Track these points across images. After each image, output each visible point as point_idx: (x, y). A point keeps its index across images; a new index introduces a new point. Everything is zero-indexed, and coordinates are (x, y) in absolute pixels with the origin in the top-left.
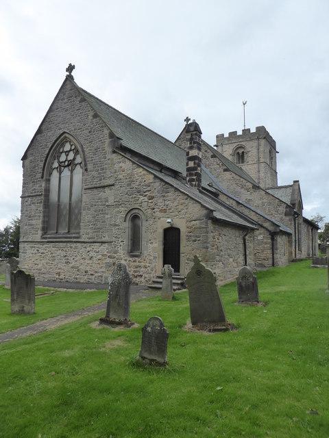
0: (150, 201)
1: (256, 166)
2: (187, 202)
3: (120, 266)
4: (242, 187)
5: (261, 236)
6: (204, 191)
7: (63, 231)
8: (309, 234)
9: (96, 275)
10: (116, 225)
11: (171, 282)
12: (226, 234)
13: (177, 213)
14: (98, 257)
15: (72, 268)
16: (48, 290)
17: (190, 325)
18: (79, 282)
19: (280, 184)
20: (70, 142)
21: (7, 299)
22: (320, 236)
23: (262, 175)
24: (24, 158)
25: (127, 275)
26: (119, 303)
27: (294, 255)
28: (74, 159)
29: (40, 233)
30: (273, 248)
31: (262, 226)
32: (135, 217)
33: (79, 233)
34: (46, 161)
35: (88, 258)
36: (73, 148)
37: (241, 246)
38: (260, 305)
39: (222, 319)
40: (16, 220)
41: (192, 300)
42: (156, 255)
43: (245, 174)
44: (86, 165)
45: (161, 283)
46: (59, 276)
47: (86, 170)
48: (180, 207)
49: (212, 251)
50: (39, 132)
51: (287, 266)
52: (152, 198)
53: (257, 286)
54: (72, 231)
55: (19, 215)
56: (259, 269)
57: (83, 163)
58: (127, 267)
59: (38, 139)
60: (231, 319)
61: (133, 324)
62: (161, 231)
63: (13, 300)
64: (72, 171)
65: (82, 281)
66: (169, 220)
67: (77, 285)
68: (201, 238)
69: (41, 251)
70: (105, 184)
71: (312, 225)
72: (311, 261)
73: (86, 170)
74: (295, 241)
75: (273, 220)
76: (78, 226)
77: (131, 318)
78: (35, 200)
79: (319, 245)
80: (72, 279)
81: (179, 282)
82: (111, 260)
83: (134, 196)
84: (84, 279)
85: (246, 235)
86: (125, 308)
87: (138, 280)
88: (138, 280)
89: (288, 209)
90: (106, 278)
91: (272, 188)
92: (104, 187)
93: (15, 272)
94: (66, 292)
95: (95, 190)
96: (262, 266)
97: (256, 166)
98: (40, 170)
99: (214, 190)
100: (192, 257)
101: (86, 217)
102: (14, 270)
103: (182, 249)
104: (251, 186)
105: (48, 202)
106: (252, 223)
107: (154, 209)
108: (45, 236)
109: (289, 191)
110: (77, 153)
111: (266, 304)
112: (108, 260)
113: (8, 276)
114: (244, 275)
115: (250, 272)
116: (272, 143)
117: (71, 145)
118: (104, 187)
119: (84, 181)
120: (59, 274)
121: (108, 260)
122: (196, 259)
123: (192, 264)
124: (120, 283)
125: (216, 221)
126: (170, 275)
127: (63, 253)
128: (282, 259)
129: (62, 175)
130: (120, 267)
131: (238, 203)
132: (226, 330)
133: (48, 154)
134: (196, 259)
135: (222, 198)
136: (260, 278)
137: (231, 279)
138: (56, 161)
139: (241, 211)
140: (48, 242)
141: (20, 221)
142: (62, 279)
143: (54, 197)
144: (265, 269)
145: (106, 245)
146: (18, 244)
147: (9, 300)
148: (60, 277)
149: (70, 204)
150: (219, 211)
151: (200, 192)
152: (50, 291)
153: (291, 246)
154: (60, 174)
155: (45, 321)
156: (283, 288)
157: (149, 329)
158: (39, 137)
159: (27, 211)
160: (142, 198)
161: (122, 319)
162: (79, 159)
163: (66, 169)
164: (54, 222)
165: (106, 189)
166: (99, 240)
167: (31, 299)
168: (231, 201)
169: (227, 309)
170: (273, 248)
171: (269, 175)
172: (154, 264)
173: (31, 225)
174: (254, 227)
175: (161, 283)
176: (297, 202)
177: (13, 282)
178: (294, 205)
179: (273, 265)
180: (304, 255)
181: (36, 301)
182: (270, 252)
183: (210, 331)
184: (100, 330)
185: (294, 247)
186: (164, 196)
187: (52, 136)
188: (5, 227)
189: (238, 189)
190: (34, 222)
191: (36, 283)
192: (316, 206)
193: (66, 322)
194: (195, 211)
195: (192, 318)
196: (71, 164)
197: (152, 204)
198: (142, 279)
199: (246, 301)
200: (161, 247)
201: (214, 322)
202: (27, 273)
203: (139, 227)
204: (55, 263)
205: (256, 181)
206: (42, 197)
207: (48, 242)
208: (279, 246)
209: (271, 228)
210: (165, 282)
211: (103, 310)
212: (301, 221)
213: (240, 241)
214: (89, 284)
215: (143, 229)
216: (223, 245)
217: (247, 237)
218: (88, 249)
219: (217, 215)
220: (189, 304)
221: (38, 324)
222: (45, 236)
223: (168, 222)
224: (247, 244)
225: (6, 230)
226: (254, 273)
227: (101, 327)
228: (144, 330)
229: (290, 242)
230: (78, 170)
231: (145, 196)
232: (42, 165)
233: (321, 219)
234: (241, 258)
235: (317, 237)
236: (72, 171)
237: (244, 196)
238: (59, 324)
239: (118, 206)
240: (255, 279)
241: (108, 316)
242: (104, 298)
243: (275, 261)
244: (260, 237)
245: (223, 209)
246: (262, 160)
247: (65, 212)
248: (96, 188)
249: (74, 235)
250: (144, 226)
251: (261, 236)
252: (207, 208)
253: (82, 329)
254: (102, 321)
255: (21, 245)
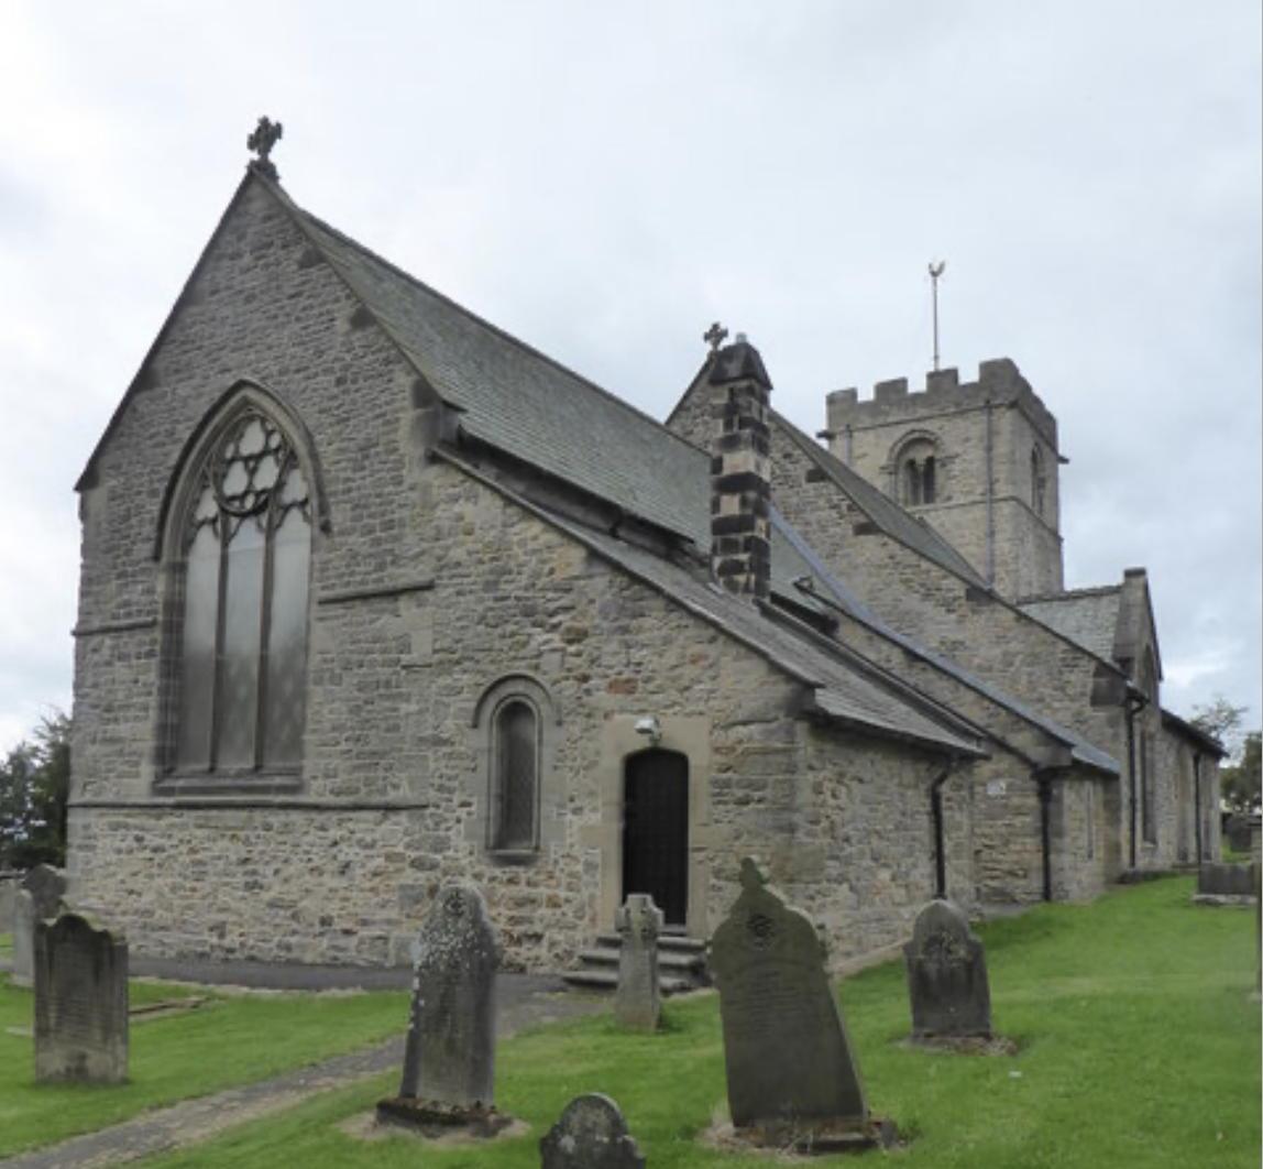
0: (572, 649)
1: (979, 512)
2: (711, 651)
3: (456, 902)
4: (927, 596)
5: (998, 782)
6: (779, 608)
7: (236, 762)
8: (1184, 778)
9: (364, 932)
10: (445, 742)
11: (653, 958)
12: (867, 777)
13: (674, 695)
14: (373, 864)
15: (272, 905)
16: (176, 992)
17: (726, 1127)
18: (297, 963)
19: (1073, 581)
20: (263, 421)
21: (21, 1026)
22: (1230, 784)
23: (1003, 546)
24: (86, 483)
25: (484, 933)
26: (451, 1045)
27: (1125, 857)
28: (280, 485)
29: (147, 770)
30: (1047, 831)
31: (1002, 746)
32: (515, 712)
33: (296, 772)
34: (170, 491)
35: (333, 866)
36: (275, 441)
37: (924, 821)
38: (995, 1051)
39: (849, 1103)
40: (54, 719)
41: (732, 1031)
42: (596, 855)
43: (937, 541)
44: (323, 509)
45: (612, 964)
46: (222, 936)
47: (326, 528)
48: (689, 672)
49: (811, 841)
50: (145, 379)
51: (1102, 899)
52: (577, 636)
53: (983, 977)
54: (273, 763)
55: (66, 702)
56: (991, 911)
57: (314, 502)
58: (484, 904)
59: (141, 408)
60: (882, 1104)
61: (505, 1122)
62: (612, 766)
63: (42, 1032)
64: (270, 532)
65: (309, 958)
66: (646, 723)
67: (291, 973)
68: (768, 793)
69: (152, 840)
70: (402, 582)
71: (1196, 741)
72: (1192, 881)
73: (326, 528)
74: (1133, 801)
75: (1047, 722)
76: (296, 746)
77: (500, 1099)
78: (130, 643)
79: (1225, 817)
80: (270, 950)
81: (684, 959)
82: (422, 878)
83: (510, 628)
84: (315, 949)
85: (941, 780)
86: (477, 1062)
87: (524, 953)
88: (524, 953)
89: (1103, 681)
90: (403, 946)
91: (1040, 599)
92: (394, 594)
93: (51, 922)
94: (246, 1000)
95: (361, 611)
96: (1005, 898)
97: (979, 512)
98: (149, 530)
99: (817, 607)
100: (735, 865)
101: (326, 708)
102: (49, 915)
103: (696, 834)
104: (960, 590)
105: (179, 653)
106: (965, 734)
107: (585, 678)
108: (167, 783)
109: (1109, 609)
110: (289, 460)
111: (1019, 1044)
112: (410, 876)
113: (25, 939)
114: (935, 934)
115: (955, 924)
116: (1040, 426)
117: (269, 434)
118: (394, 594)
119: (317, 571)
120: (220, 929)
121: (410, 876)
122: (749, 875)
123: (734, 891)
124: (455, 966)
125: (828, 727)
126: (649, 935)
127: (236, 851)
128: (1080, 871)
129: (234, 546)
130: (456, 903)
131: (912, 656)
132: (866, 1145)
133: (178, 469)
134: (749, 875)
135: (849, 636)
136: (997, 945)
137: (886, 948)
138: (209, 494)
139: (922, 687)
140: (179, 806)
141: (70, 727)
142: (231, 951)
143: (200, 631)
144: (1014, 912)
145: (403, 817)
146: (64, 814)
147: (30, 1032)
148: (227, 942)
149: (264, 660)
150: (838, 685)
151: (766, 612)
152: (185, 994)
153: (1114, 820)
154: (225, 545)
155: (166, 1112)
156: (1083, 985)
157: (568, 1142)
158: (142, 402)
159: (95, 686)
160: (540, 636)
161: (465, 1103)
162: (297, 488)
163: (249, 526)
164: (199, 727)
165: (403, 603)
166: (376, 799)
167: (114, 1027)
168: (885, 647)
169: (867, 1064)
170: (1047, 831)
171: (1030, 546)
172: (585, 894)
173: (112, 741)
174: (972, 747)
175: (612, 964)
176: (1137, 653)
177: (45, 958)
178: (1126, 662)
179: (1047, 894)
180: (1164, 854)
181: (134, 1033)
182: (1033, 843)
183: (802, 1149)
184: (379, 1146)
185: (1125, 825)
186: (625, 630)
187: (193, 397)
188: (12, 748)
189: (913, 602)
190: (123, 729)
191: (132, 965)
192: (1209, 668)
193: (249, 1114)
194: (745, 685)
195: (734, 1099)
196: (268, 506)
197: (577, 661)
198: (542, 951)
199: (943, 1033)
200: (615, 828)
201: (817, 1114)
202: (98, 927)
203: (529, 749)
204: (205, 887)
205: (982, 570)
206: (158, 634)
207: (179, 806)
208: (1068, 821)
209: (1039, 754)
210: (631, 962)
211: (391, 1069)
212: (1154, 725)
213: (919, 802)
214: (335, 970)
215: (546, 757)
216: (853, 820)
217: (945, 789)
218: (334, 833)
219: (831, 702)
220: (718, 1049)
221: (140, 1121)
222: (167, 783)
223: (643, 731)
224: (946, 814)
225: (19, 760)
226: (974, 927)
227: (382, 1135)
228: (548, 1146)
229: (1112, 807)
230: (296, 529)
231: (555, 627)
232: (154, 507)
233: (1232, 717)
234: (923, 870)
235: (1216, 787)
236: (270, 532)
237: (935, 630)
238: (220, 1122)
239: (444, 667)
240: (977, 952)
241: (408, 1089)
242: (395, 1022)
243: (1055, 879)
244: (997, 789)
245: (853, 678)
246: (1003, 490)
247: (245, 691)
248: (364, 597)
249: (278, 781)
250: (550, 743)
251: (998, 782)
252: (791, 677)
253: (310, 1141)
254: (389, 1111)
255: (75, 820)
